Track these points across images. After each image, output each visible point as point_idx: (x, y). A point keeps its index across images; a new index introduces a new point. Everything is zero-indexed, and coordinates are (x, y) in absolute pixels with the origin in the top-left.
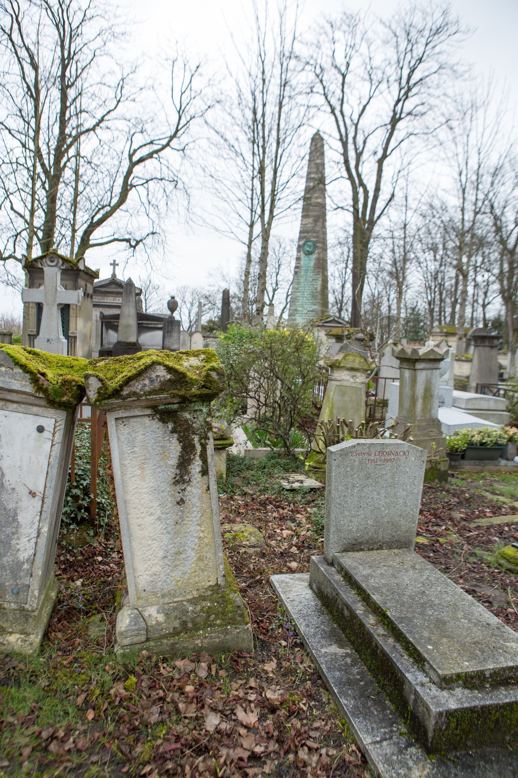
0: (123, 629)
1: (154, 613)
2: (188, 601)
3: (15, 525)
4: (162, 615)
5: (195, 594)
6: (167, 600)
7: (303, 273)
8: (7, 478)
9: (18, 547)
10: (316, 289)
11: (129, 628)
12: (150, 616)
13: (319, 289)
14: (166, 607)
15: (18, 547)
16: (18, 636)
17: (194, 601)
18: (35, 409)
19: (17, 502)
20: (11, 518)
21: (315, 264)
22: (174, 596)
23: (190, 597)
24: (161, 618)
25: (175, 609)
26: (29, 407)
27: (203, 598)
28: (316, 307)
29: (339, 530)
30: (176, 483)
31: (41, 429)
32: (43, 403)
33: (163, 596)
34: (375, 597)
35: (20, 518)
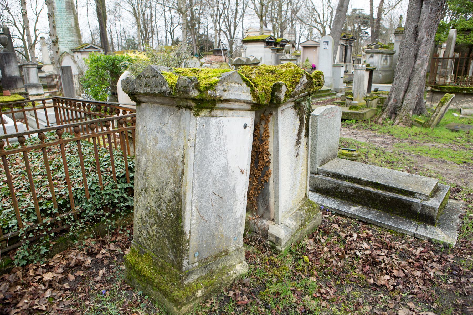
0: (284, 236)
1: (290, 222)
2: (298, 210)
3: (234, 196)
4: (293, 221)
5: (300, 205)
6: (291, 213)
7: (58, 13)
8: (230, 165)
9: (236, 210)
10: (71, 25)
11: (286, 234)
12: (289, 224)
13: (73, 24)
14: (292, 217)
15: (236, 210)
16: (239, 265)
17: (300, 209)
18: (242, 113)
19: (235, 180)
20: (233, 192)
21: (66, 7)
22: (293, 209)
23: (298, 207)
24: (294, 223)
25: (296, 216)
26: (239, 111)
27: (303, 206)
28: (73, 38)
29: (319, 156)
30: (296, 145)
31: (245, 126)
32: (249, 107)
33: (289, 212)
34: (365, 179)
35: (237, 191)
